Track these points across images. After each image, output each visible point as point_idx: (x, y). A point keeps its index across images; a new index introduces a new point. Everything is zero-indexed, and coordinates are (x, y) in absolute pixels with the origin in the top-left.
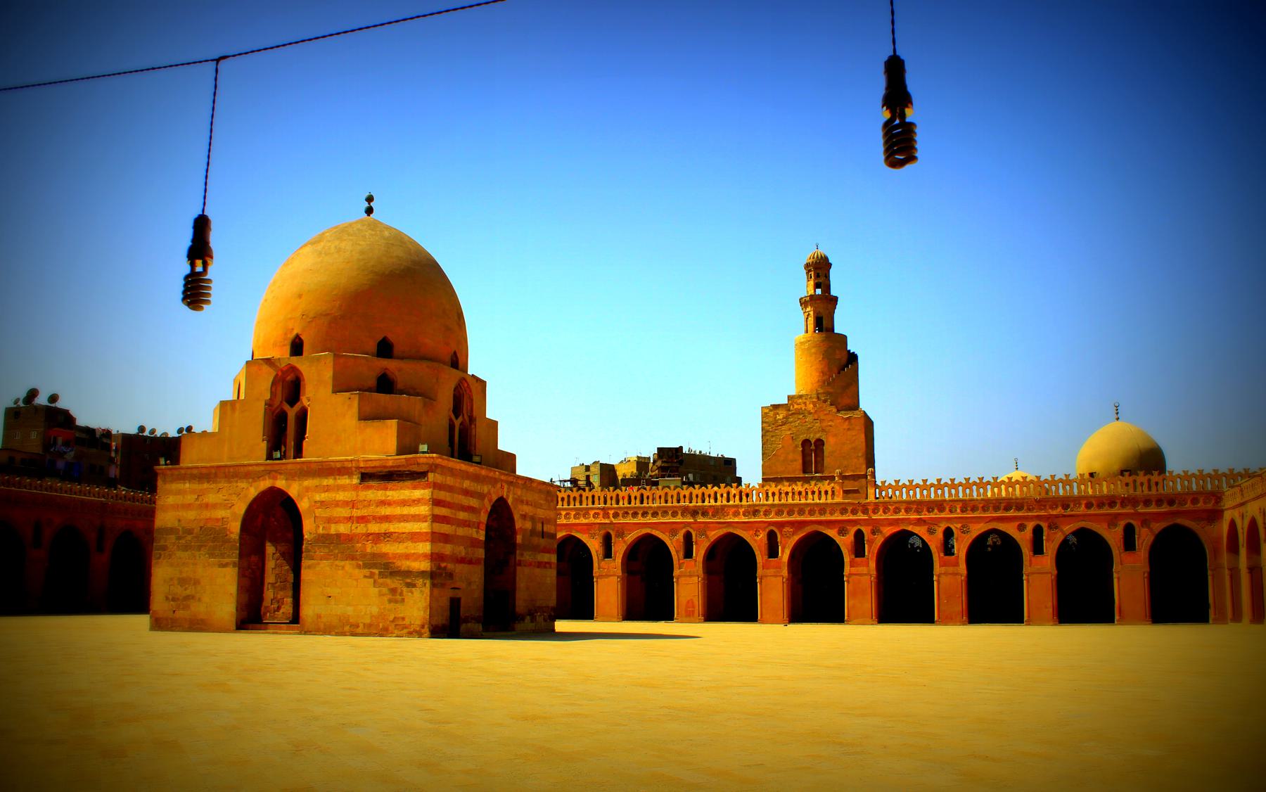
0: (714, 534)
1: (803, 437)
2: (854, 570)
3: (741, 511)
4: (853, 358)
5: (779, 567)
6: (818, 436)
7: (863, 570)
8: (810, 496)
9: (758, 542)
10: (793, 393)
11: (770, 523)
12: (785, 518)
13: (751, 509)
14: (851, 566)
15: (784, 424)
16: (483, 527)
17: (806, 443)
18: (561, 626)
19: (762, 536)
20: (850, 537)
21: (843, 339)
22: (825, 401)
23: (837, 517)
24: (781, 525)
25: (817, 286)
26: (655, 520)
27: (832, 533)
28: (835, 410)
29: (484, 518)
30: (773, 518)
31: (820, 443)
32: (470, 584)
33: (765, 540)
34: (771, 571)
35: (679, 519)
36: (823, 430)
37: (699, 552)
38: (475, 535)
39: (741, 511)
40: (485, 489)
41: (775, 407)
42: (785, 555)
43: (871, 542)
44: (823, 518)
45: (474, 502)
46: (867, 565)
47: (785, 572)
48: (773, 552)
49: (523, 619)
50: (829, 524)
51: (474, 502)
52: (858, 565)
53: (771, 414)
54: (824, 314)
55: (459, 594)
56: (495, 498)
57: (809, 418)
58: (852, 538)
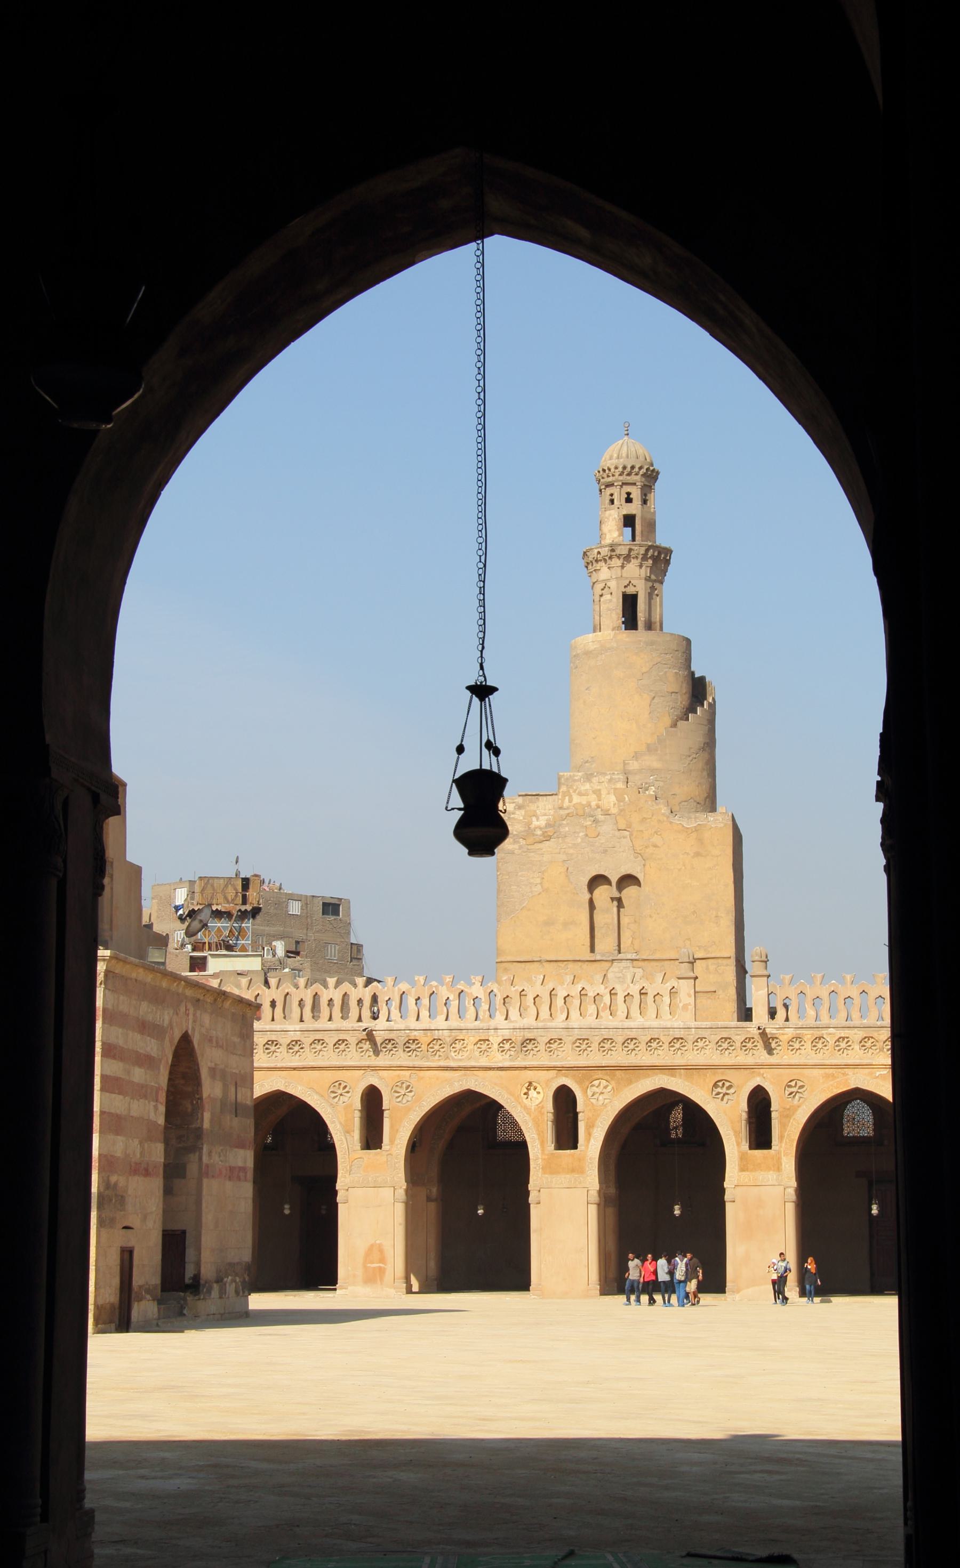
2: (746, 1177)
3: (495, 1040)
4: (698, 690)
5: (577, 1169)
7: (771, 1176)
8: (621, 1008)
9: (531, 1116)
11: (559, 1069)
12: (595, 1058)
13: (519, 1037)
14: (743, 1169)
15: (548, 838)
16: (162, 1097)
17: (597, 881)
18: (259, 1301)
22: (642, 789)
23: (710, 1056)
25: (629, 521)
28: (664, 810)
29: (163, 1079)
32: (145, 1218)
33: (549, 1106)
34: (563, 1179)
37: (399, 1131)
38: (152, 1116)
39: (495, 1040)
40: (165, 1017)
43: (788, 1114)
44: (679, 1060)
45: (150, 1046)
46: (779, 1169)
47: (591, 1179)
48: (566, 1134)
49: (209, 1292)
50: (690, 1069)
51: (150, 1046)
54: (641, 589)
55: (130, 1240)
56: (177, 1035)
58: (744, 1106)
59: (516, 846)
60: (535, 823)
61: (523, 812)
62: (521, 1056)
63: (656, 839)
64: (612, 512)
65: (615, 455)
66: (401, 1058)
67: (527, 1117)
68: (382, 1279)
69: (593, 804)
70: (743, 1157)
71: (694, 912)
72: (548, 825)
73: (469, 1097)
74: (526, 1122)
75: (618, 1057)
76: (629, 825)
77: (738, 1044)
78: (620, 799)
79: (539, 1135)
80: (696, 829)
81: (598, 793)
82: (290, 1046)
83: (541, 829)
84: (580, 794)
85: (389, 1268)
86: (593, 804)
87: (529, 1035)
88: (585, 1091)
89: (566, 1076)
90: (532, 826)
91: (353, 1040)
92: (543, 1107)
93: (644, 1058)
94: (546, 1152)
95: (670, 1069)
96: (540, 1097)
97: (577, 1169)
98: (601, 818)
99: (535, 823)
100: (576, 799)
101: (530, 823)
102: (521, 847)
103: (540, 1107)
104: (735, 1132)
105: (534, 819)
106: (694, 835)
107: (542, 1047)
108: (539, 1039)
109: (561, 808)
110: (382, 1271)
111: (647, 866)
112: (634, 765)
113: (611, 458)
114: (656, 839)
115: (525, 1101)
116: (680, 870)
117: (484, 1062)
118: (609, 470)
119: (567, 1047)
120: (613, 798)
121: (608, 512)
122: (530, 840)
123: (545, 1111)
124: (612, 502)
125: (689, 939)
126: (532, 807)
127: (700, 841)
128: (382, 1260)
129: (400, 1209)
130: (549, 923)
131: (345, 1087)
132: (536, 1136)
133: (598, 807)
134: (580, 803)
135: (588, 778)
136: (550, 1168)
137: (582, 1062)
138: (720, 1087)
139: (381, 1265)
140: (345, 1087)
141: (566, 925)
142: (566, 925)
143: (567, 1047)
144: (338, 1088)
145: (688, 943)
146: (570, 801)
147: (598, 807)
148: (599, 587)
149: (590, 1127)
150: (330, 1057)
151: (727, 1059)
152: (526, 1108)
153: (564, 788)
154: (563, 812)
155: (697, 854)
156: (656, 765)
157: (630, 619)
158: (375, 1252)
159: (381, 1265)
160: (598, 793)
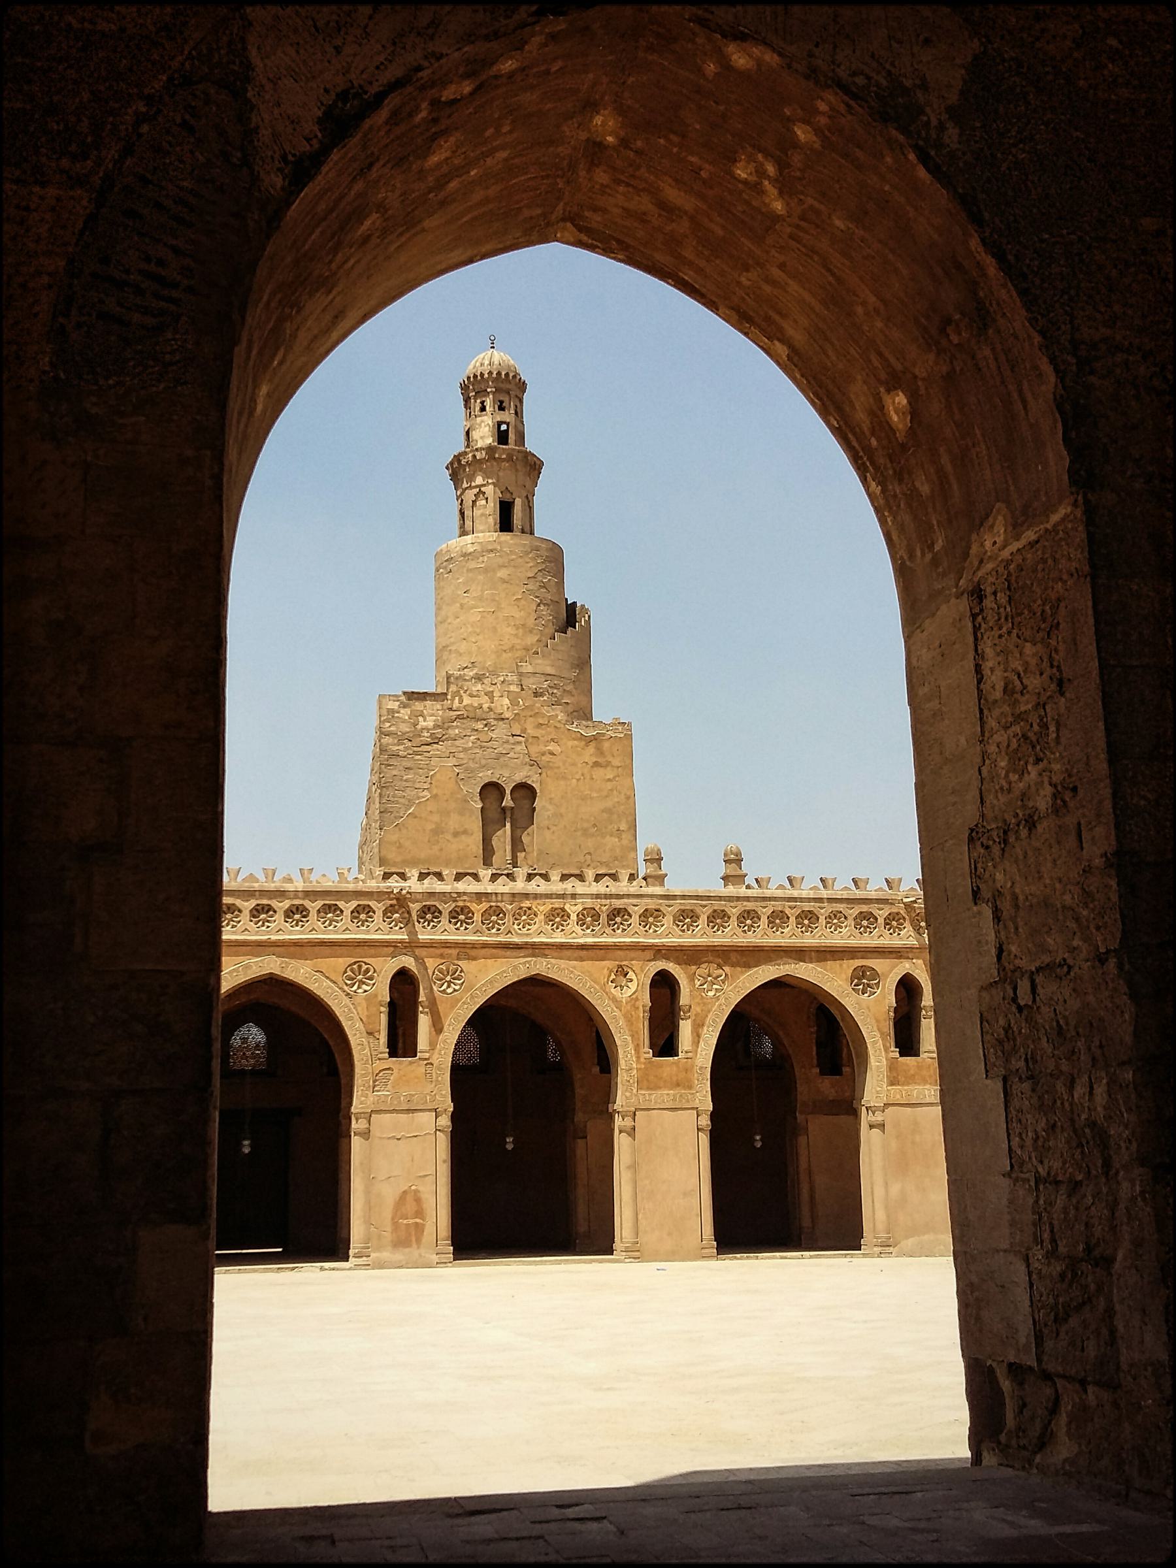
0: (488, 978)
1: (486, 776)
2: (897, 1093)
5: (683, 1083)
6: (519, 777)
10: (452, 669)
11: (659, 952)
12: (700, 936)
13: (604, 907)
17: (491, 790)
19: (636, 987)
20: (886, 997)
21: (553, 559)
23: (845, 936)
24: (691, 956)
26: (295, 933)
27: (831, 980)
30: (668, 934)
31: (525, 791)
33: (646, 999)
34: (666, 1095)
35: (378, 930)
36: (534, 763)
41: (412, 696)
42: (699, 1043)
47: (704, 1099)
52: (910, 1079)
53: (405, 713)
57: (500, 731)
59: (401, 747)
60: (422, 723)
61: (408, 711)
62: (608, 930)
63: (552, 747)
64: (485, 418)
65: (487, 362)
66: (445, 932)
67: (617, 1013)
68: (418, 1241)
69: (485, 706)
70: (892, 1066)
71: (595, 825)
72: (436, 726)
73: (536, 988)
74: (615, 1017)
75: (731, 935)
76: (524, 730)
77: (881, 921)
78: (514, 703)
79: (632, 1036)
80: (595, 738)
81: (490, 695)
82: (289, 913)
83: (428, 730)
84: (471, 696)
85: (429, 1229)
86: (485, 706)
87: (618, 903)
88: (692, 978)
89: (668, 959)
90: (419, 727)
91: (378, 907)
92: (637, 999)
93: (762, 936)
94: (642, 1060)
95: (799, 954)
96: (633, 986)
97: (683, 1083)
98: (493, 722)
99: (422, 723)
100: (467, 701)
101: (415, 725)
102: (407, 748)
103: (633, 999)
104: (882, 1034)
105: (421, 719)
106: (593, 744)
107: (635, 920)
108: (631, 909)
109: (450, 709)
110: (419, 1228)
111: (544, 775)
112: (527, 668)
113: (482, 365)
114: (552, 747)
115: (613, 990)
116: (578, 780)
117: (559, 938)
118: (482, 374)
119: (668, 921)
120: (506, 701)
121: (479, 419)
122: (417, 741)
123: (640, 1004)
124: (483, 409)
125: (589, 853)
126: (418, 706)
127: (600, 752)
128: (420, 1213)
129: (443, 1143)
130: (437, 831)
131: (367, 971)
132: (629, 1038)
133: (490, 709)
134: (471, 705)
135: (479, 678)
136: (646, 1081)
137: (687, 940)
138: (863, 979)
139: (418, 1220)
140: (367, 971)
141: (456, 834)
142: (456, 834)
143: (668, 921)
144: (359, 974)
145: (588, 857)
146: (461, 701)
147: (490, 709)
148: (470, 495)
149: (698, 1027)
150: (343, 930)
151: (867, 941)
152: (614, 1000)
153: (453, 688)
154: (452, 713)
155: (596, 764)
156: (549, 670)
157: (505, 525)
158: (409, 1202)
159: (418, 1220)
160: (490, 695)
